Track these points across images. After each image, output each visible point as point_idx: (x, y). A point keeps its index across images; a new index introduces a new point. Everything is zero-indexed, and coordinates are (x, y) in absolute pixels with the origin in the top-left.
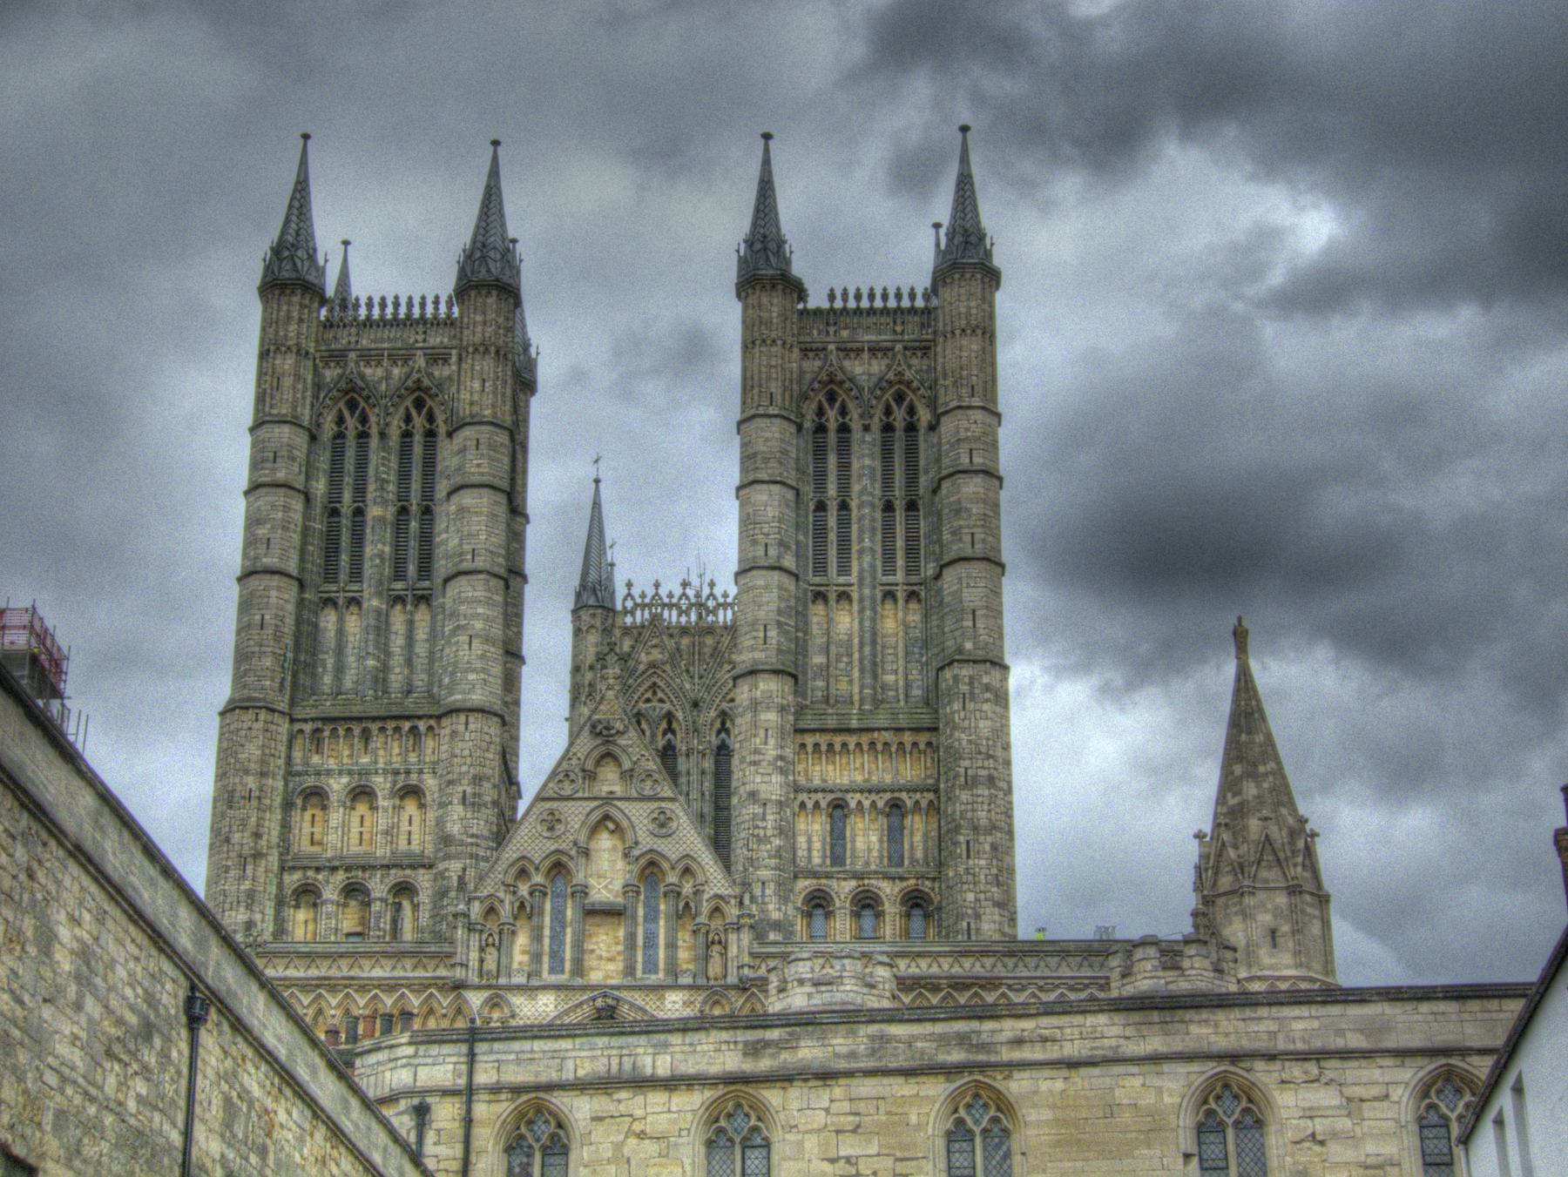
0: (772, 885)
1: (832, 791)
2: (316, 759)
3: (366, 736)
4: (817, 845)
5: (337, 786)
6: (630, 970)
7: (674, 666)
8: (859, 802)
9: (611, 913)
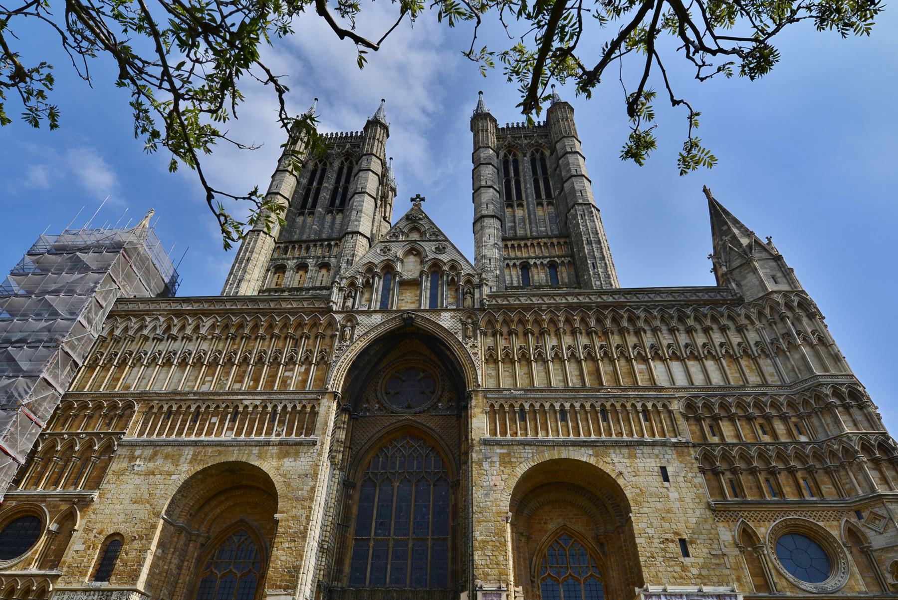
0: (495, 288)
1: (521, 259)
3: (308, 249)
8: (535, 263)
9: (415, 284)
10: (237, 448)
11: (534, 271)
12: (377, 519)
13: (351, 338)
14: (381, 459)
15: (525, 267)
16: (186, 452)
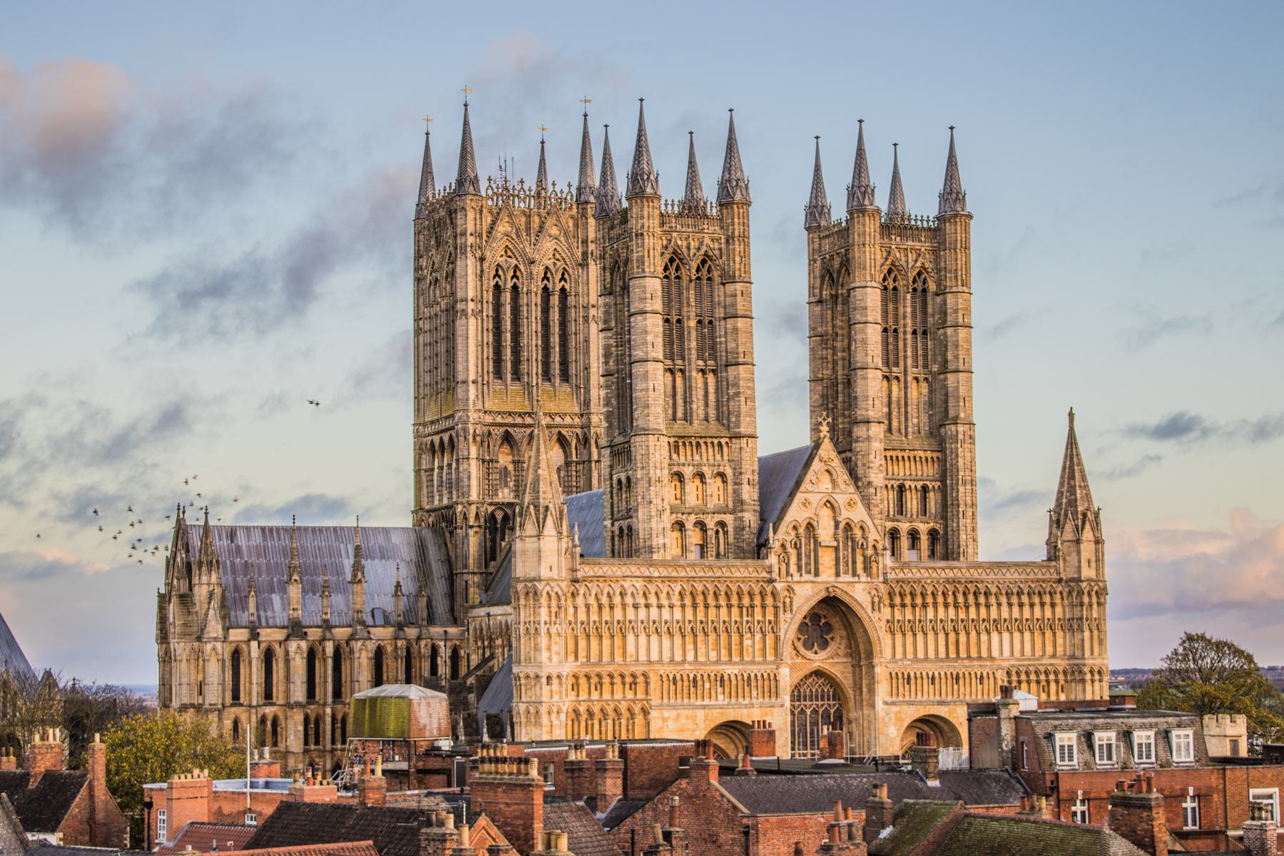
2: (675, 456)
3: (698, 445)
4: (891, 506)
5: (688, 471)
6: (838, 574)
7: (518, 236)
11: (908, 493)
13: (791, 611)
15: (901, 489)
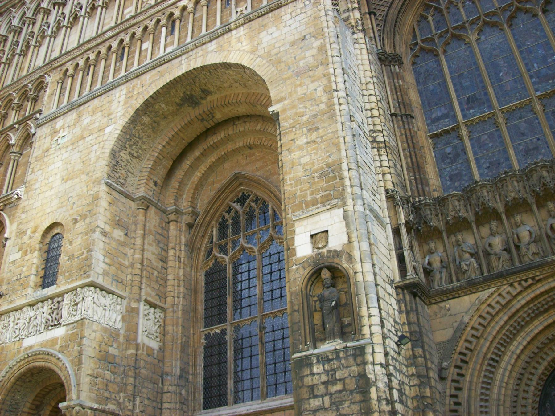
10: (184, 57)
12: (458, 96)
14: (430, 19)
16: (117, 95)
